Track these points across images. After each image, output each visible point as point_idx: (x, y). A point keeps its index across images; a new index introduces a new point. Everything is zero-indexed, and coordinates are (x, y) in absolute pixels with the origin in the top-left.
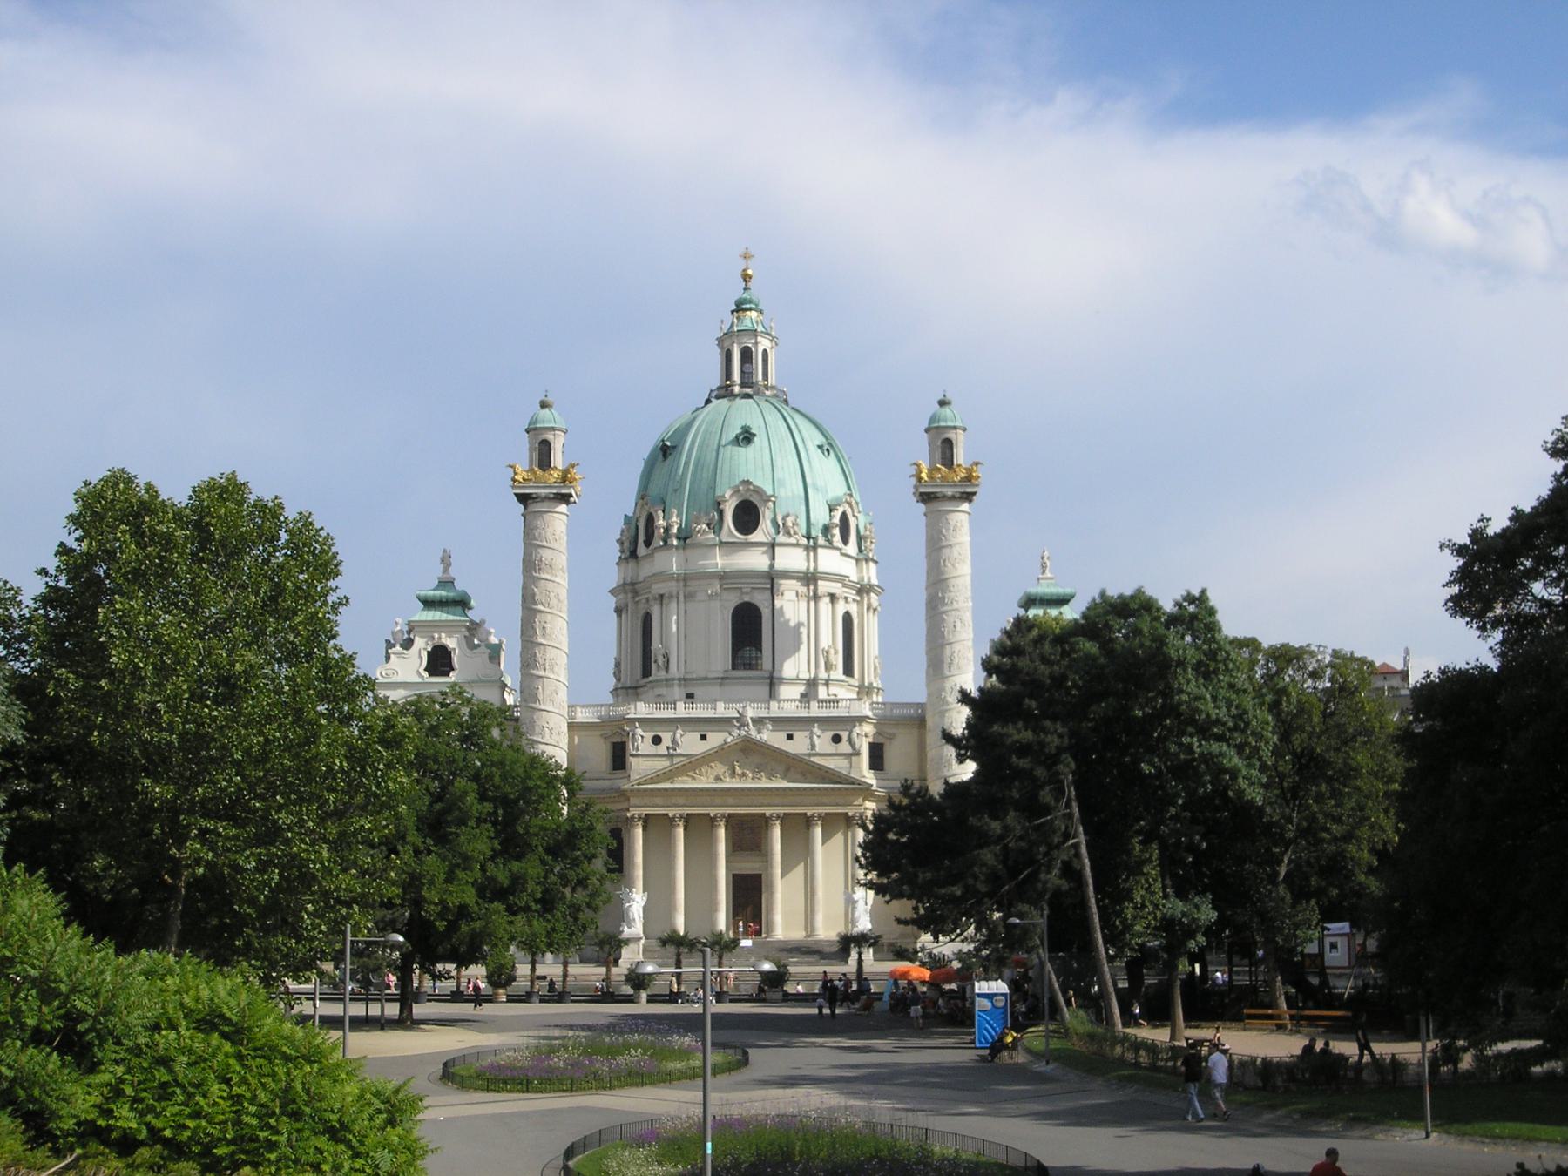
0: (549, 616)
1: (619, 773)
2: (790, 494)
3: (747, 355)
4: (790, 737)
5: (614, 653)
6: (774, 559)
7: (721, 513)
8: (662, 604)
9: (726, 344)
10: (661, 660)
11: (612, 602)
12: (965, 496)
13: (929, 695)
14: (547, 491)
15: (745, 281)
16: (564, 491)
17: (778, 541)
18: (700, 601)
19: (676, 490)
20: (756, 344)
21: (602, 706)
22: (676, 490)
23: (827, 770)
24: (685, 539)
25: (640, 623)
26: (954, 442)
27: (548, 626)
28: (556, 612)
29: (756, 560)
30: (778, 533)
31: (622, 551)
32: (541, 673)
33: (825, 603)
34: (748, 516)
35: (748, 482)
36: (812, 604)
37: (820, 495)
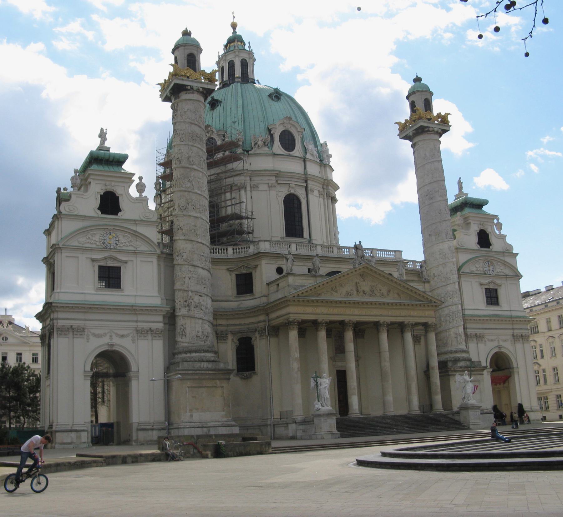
0: (201, 174)
1: (248, 297)
6: (305, 168)
7: (272, 136)
9: (230, 57)
12: (442, 132)
14: (199, 85)
18: (261, 191)
19: (234, 122)
22: (234, 122)
24: (248, 151)
28: (204, 172)
29: (295, 167)
30: (306, 153)
35: (290, 119)
36: (326, 200)
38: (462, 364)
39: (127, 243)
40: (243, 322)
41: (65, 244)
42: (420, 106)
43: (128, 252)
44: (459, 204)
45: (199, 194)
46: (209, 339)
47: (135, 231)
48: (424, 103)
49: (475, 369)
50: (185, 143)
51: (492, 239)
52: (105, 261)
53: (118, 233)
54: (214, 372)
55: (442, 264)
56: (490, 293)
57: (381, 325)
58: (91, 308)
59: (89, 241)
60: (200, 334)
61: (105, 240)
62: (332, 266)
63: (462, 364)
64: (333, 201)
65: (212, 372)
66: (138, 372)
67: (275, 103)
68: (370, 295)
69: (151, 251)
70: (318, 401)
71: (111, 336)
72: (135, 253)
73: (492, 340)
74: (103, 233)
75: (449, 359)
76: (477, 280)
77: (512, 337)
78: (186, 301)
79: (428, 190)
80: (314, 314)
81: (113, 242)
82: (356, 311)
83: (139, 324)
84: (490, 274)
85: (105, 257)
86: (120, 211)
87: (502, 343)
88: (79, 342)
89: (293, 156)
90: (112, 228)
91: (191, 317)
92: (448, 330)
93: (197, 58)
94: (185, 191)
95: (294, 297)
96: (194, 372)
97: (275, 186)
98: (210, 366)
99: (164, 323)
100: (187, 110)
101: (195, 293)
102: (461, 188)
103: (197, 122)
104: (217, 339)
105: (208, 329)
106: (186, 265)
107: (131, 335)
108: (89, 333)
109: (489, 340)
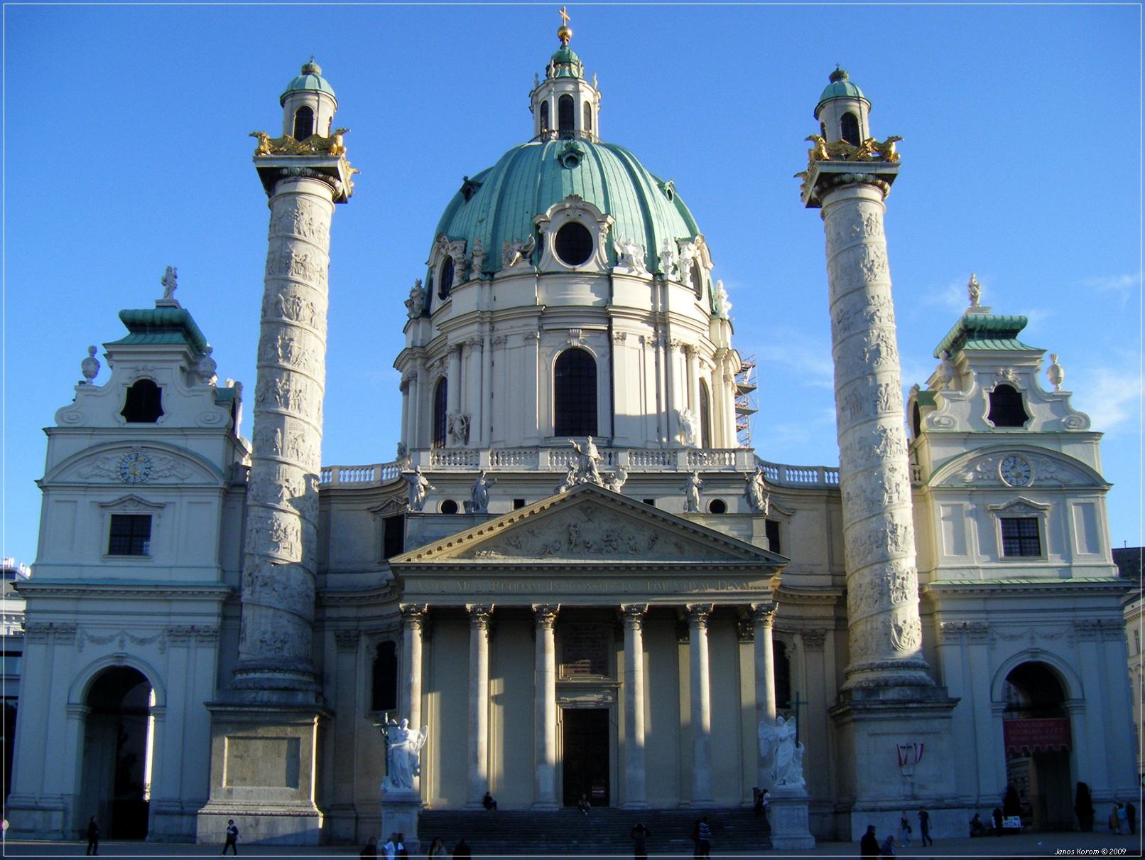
2: (628, 221)
3: (567, 106)
4: (651, 502)
5: (398, 438)
6: (611, 295)
7: (541, 239)
8: (461, 360)
9: (541, 98)
10: (457, 427)
11: (398, 377)
13: (844, 451)
14: (304, 165)
15: (562, 39)
16: (325, 164)
17: (614, 272)
18: (510, 349)
19: (481, 221)
20: (577, 92)
21: (372, 467)
23: (717, 538)
24: (492, 274)
25: (431, 396)
26: (859, 118)
27: (295, 344)
28: (307, 327)
31: (413, 311)
32: (282, 410)
33: (678, 356)
37: (667, 229)
39: (166, 472)
40: (384, 613)
41: (54, 480)
42: (835, 132)
43: (166, 488)
44: (958, 334)
45: (290, 370)
47: (179, 449)
49: (924, 705)
50: (274, 277)
51: (1031, 407)
52: (122, 505)
53: (151, 454)
54: (278, 710)
56: (1019, 528)
58: (84, 591)
59: (97, 471)
60: (268, 636)
61: (126, 468)
63: (891, 694)
65: (274, 710)
66: (165, 706)
67: (565, 172)
68: (599, 552)
70: (387, 775)
71: (122, 642)
72: (177, 488)
73: (1012, 637)
74: (123, 457)
75: (864, 684)
78: (250, 575)
79: (841, 311)
80: (459, 594)
81: (140, 468)
83: (173, 618)
85: (121, 499)
86: (161, 413)
87: (1041, 644)
88: (63, 652)
89: (582, 273)
90: (139, 445)
91: (254, 605)
92: (869, 619)
94: (266, 366)
96: (237, 709)
97: (535, 337)
98: (275, 697)
99: (224, 617)
100: (285, 212)
101: (264, 559)
102: (973, 297)
103: (300, 233)
104: (337, 645)
105: (288, 626)
106: (255, 506)
107: (160, 639)
108: (84, 637)
109: (1004, 637)
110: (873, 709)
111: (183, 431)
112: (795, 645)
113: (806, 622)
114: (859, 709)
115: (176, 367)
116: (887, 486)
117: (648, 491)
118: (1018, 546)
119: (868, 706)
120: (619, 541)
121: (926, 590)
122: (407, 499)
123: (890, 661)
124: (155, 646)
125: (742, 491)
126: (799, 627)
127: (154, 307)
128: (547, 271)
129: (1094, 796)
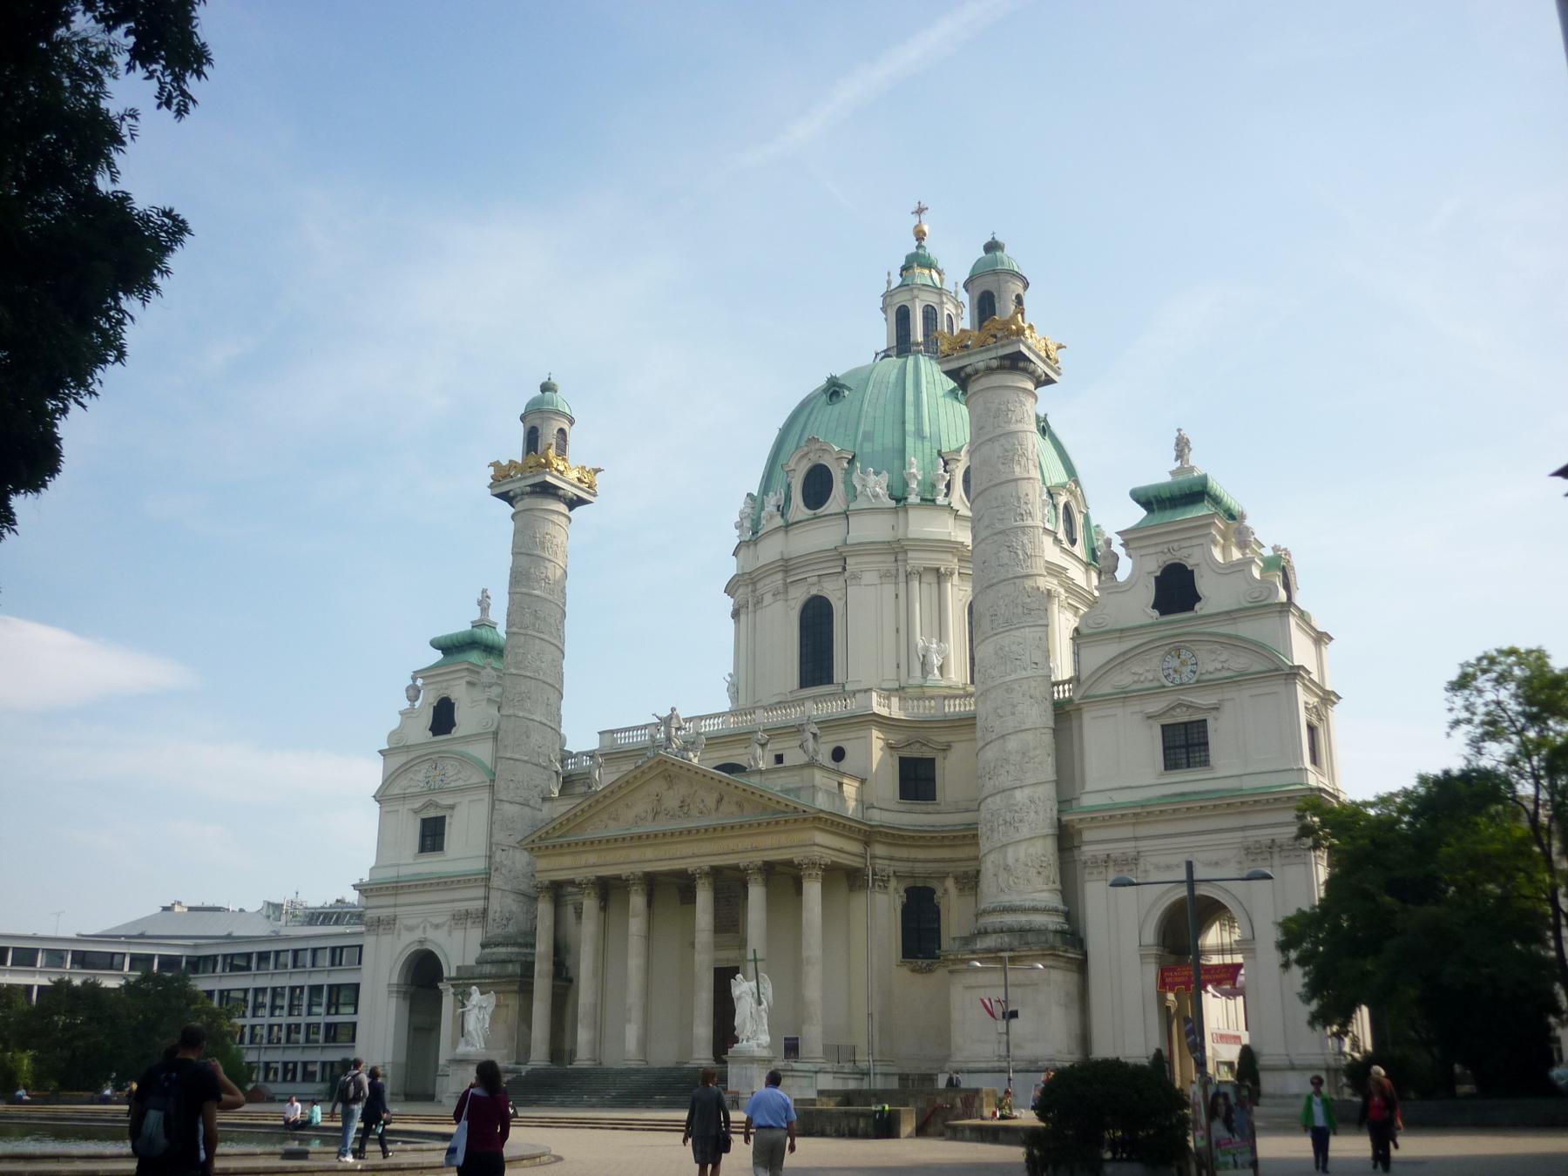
0: (522, 639)
3: (903, 317)
6: (848, 533)
7: (789, 486)
12: (1007, 363)
14: (523, 483)
15: (917, 240)
16: (537, 479)
20: (913, 299)
28: (530, 632)
34: (818, 486)
36: (902, 586)
38: (990, 942)
45: (514, 675)
46: (511, 922)
48: (976, 306)
51: (1203, 585)
54: (492, 981)
55: (982, 694)
56: (1186, 734)
57: (693, 874)
58: (397, 887)
60: (497, 915)
62: (716, 755)
63: (990, 942)
64: (942, 578)
69: (483, 782)
71: (424, 928)
76: (1137, 708)
77: (1243, 852)
82: (649, 853)
83: (455, 904)
84: (1181, 684)
88: (386, 940)
89: (820, 517)
90: (437, 756)
93: (540, 431)
95: (533, 841)
102: (1180, 455)
105: (512, 904)
107: (448, 923)
110: (965, 959)
111: (466, 739)
112: (946, 890)
113: (959, 863)
114: (951, 960)
115: (463, 682)
116: (999, 711)
117: (778, 746)
118: (1184, 756)
119: (959, 957)
120: (691, 806)
121: (1065, 818)
122: (568, 782)
123: (992, 906)
124: (446, 928)
125: (800, 742)
126: (951, 870)
127: (470, 628)
128: (795, 520)
129: (1263, 1061)
